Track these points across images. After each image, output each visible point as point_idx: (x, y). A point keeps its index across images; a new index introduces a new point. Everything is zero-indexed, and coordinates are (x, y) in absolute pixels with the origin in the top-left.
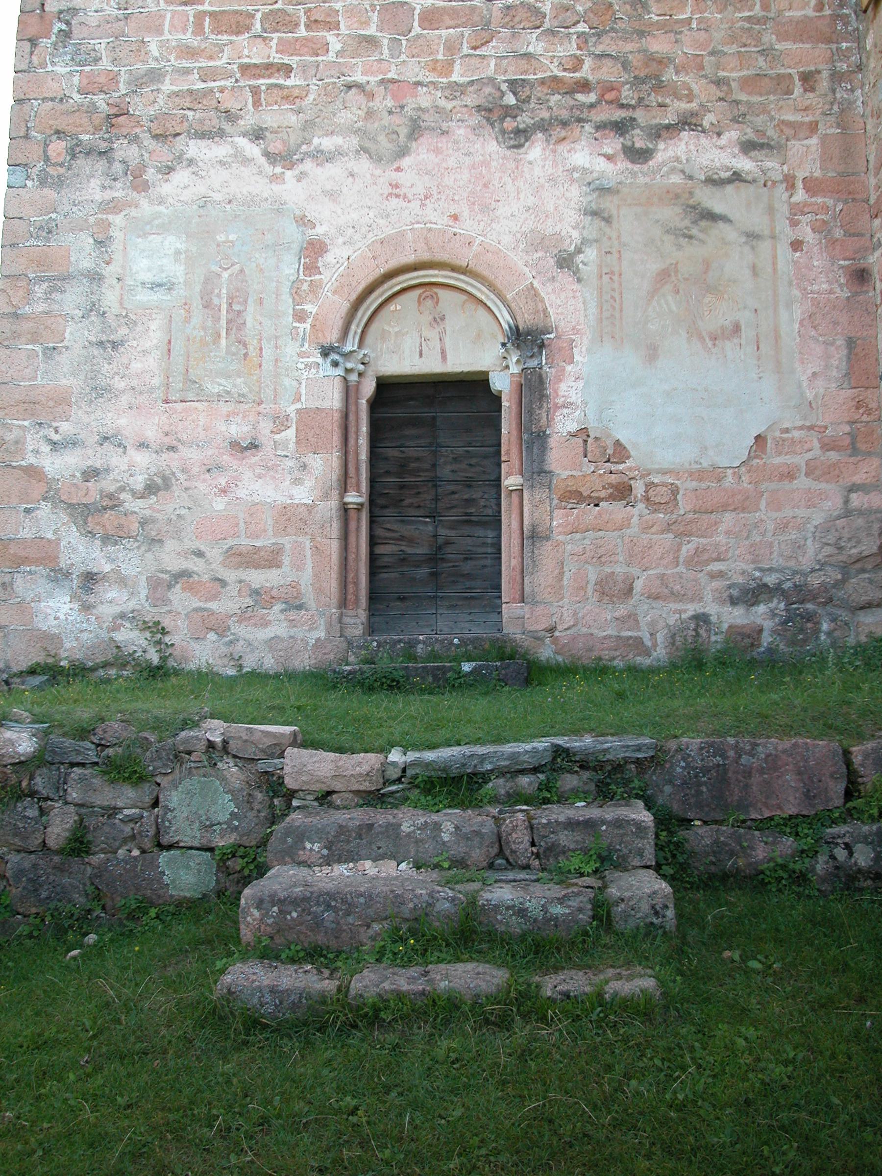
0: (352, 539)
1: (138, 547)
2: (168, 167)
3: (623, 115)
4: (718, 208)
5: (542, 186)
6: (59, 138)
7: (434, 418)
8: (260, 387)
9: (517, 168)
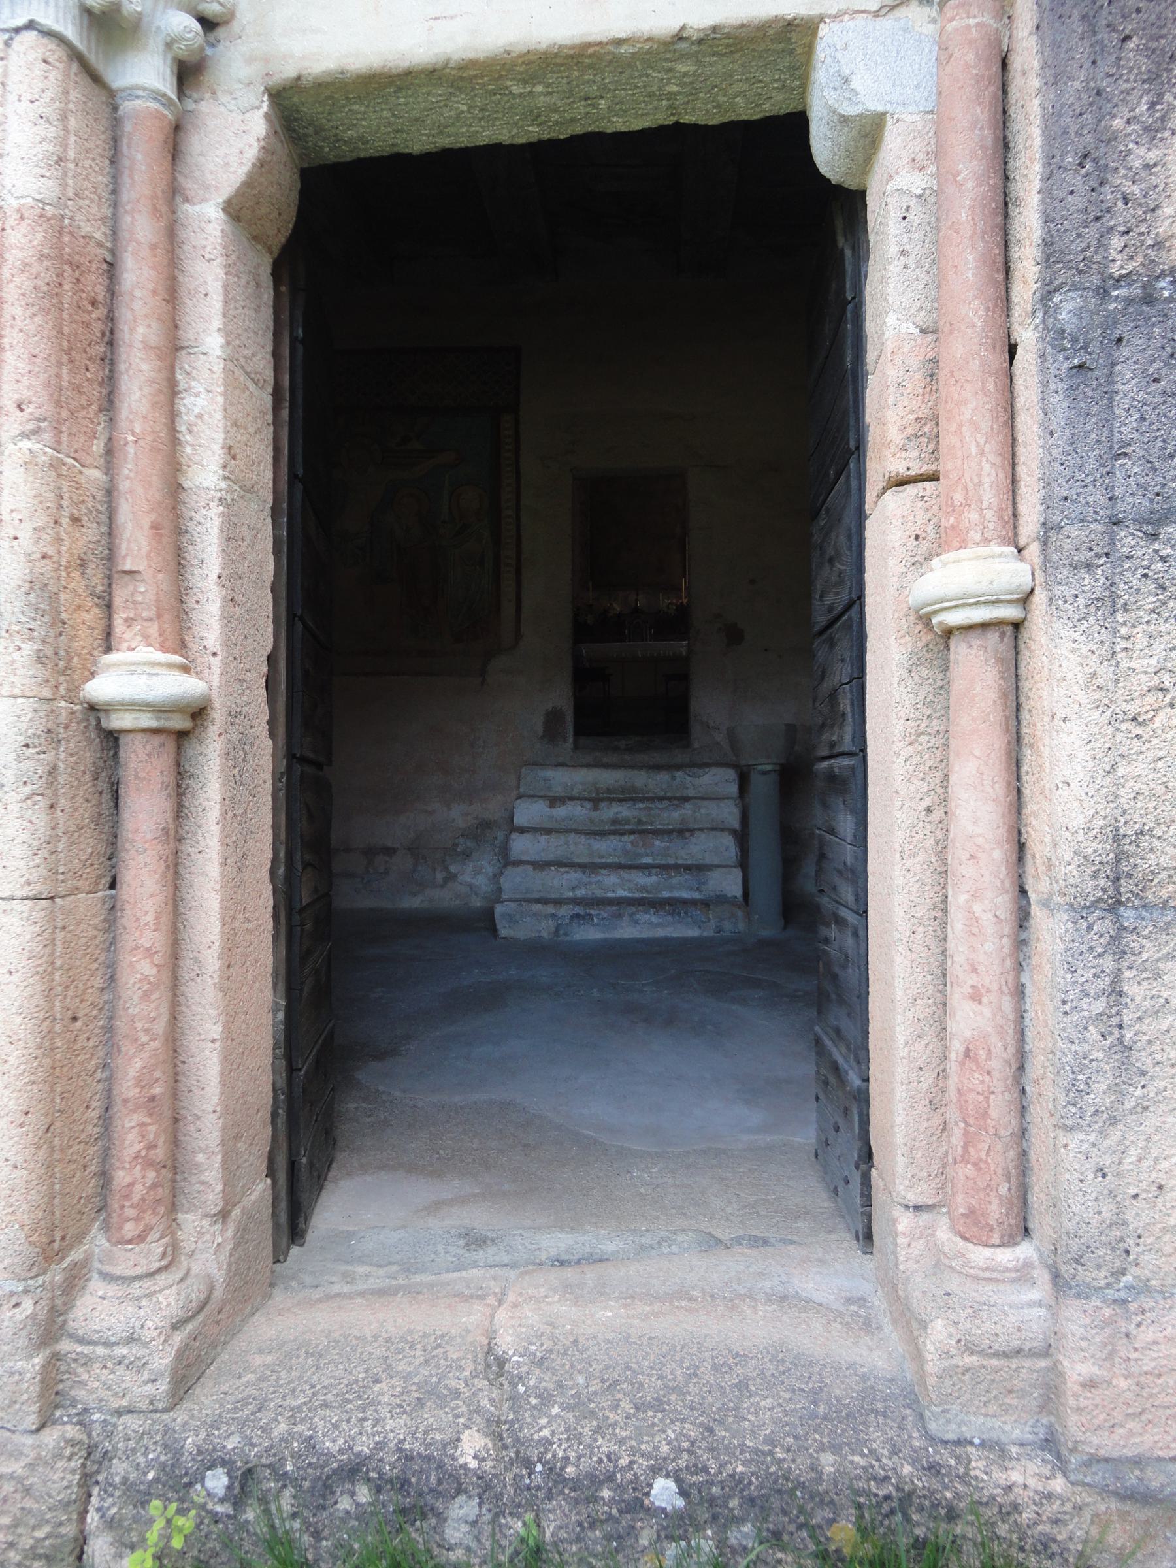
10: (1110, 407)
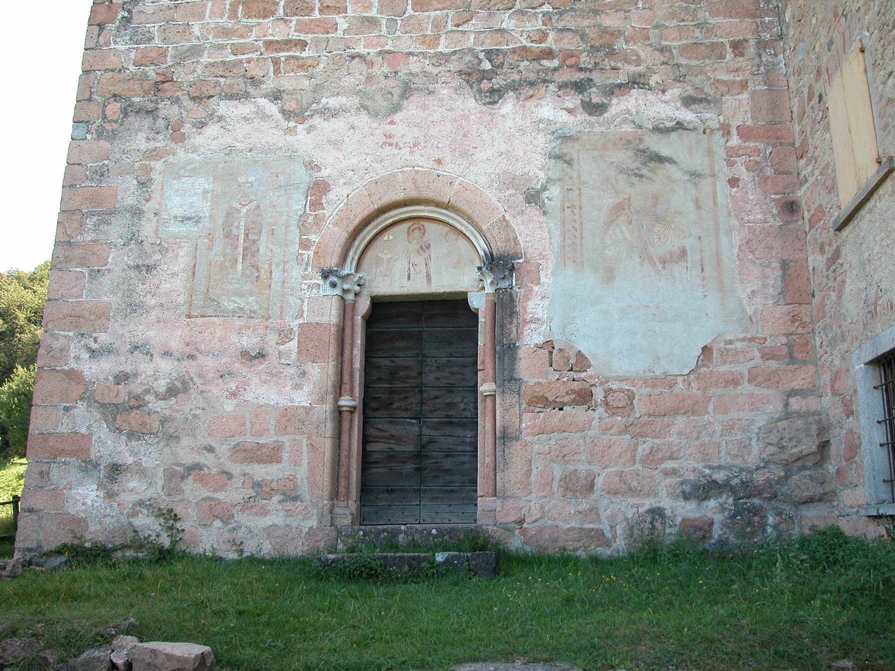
0: (345, 438)
1: (158, 443)
2: (201, 122)
3: (582, 77)
4: (664, 152)
5: (513, 135)
6: (116, 101)
7: (421, 332)
8: (268, 304)
9: (492, 120)
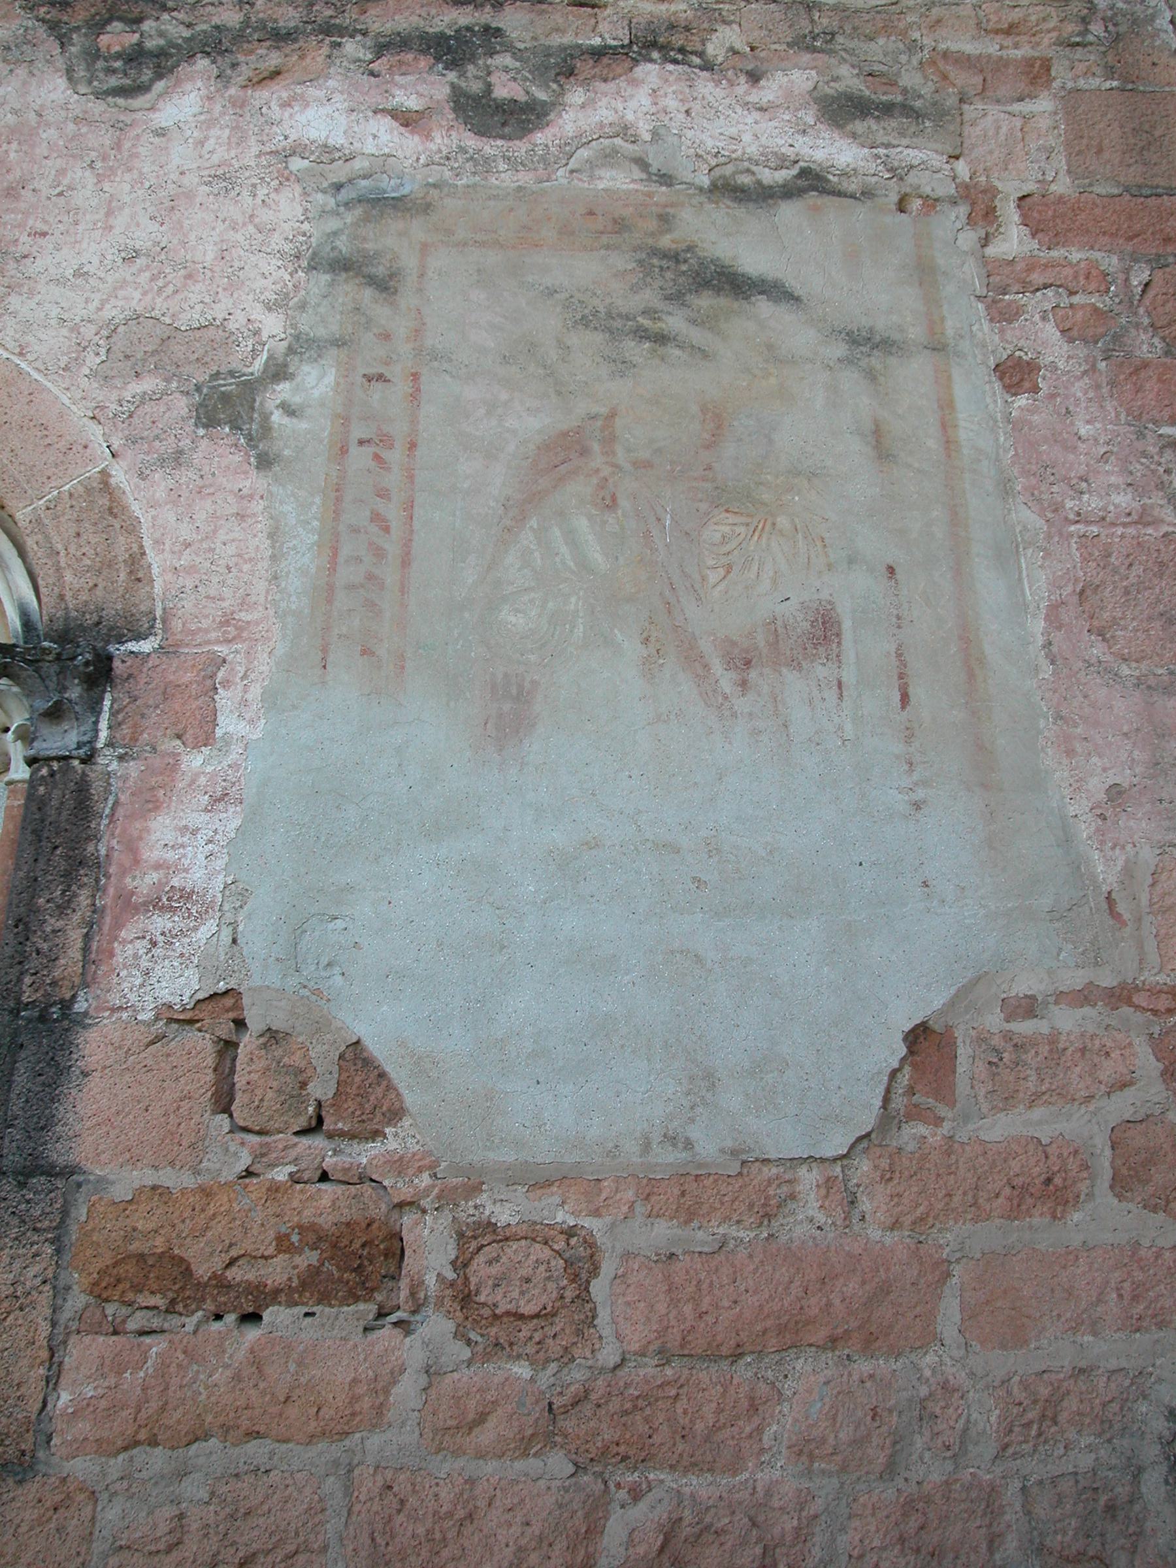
3: (463, 21)
4: (753, 261)
5: (190, 195)
9: (118, 146)
10: (9, 1091)
